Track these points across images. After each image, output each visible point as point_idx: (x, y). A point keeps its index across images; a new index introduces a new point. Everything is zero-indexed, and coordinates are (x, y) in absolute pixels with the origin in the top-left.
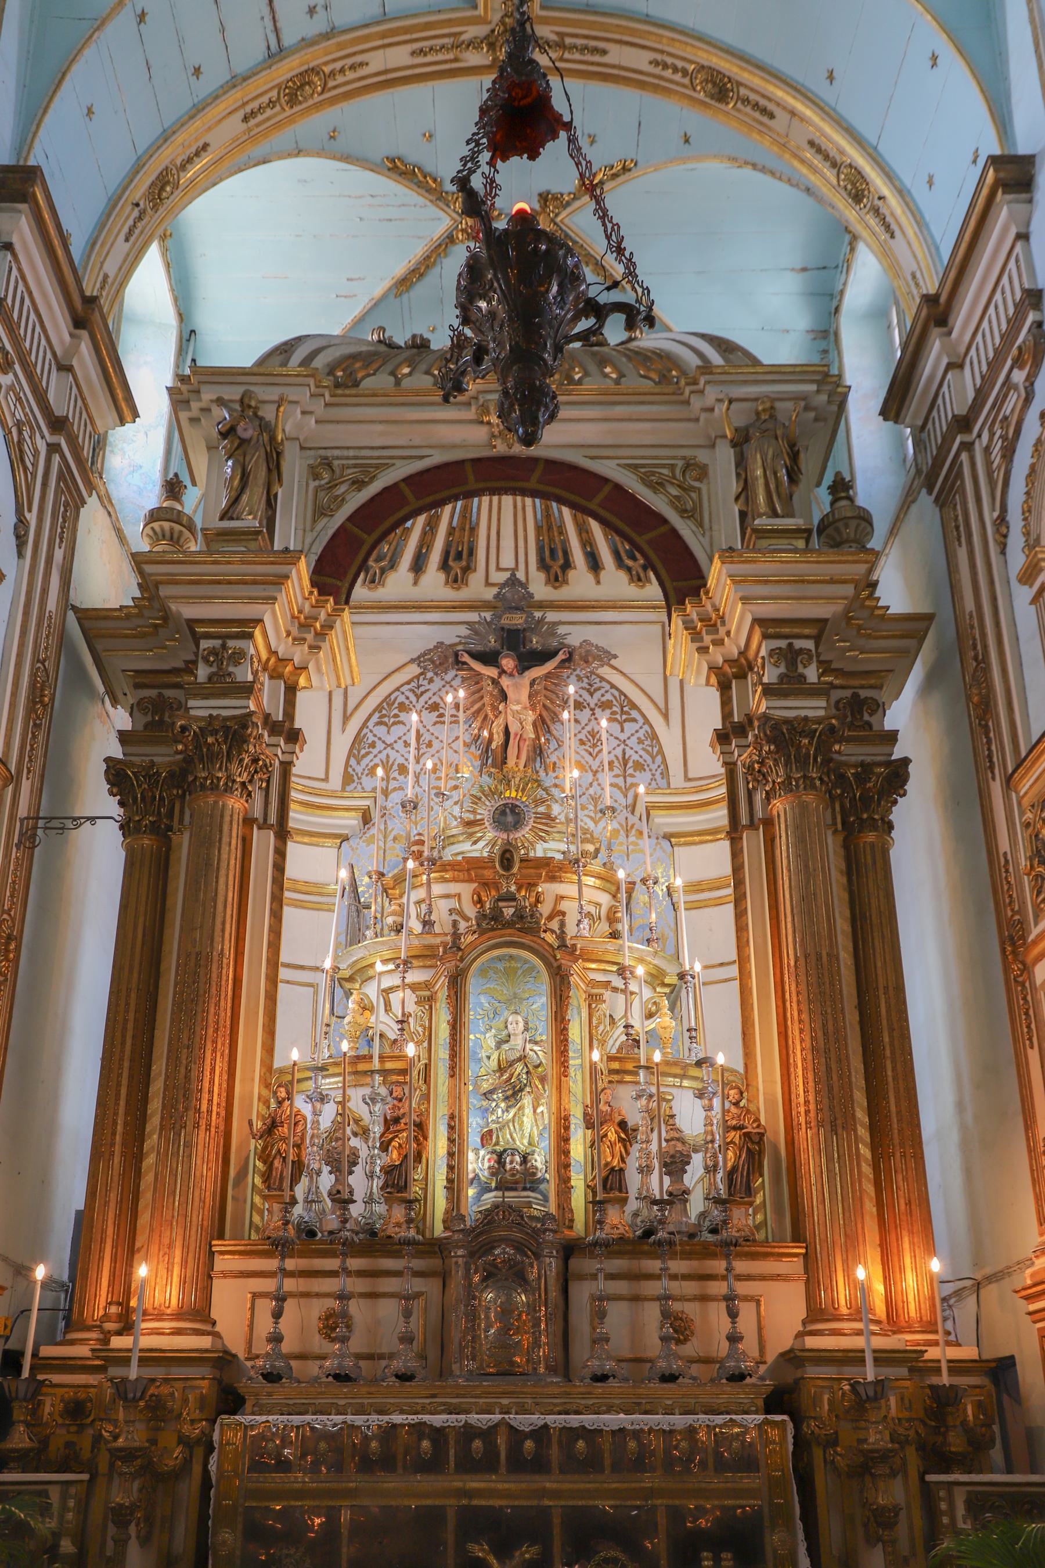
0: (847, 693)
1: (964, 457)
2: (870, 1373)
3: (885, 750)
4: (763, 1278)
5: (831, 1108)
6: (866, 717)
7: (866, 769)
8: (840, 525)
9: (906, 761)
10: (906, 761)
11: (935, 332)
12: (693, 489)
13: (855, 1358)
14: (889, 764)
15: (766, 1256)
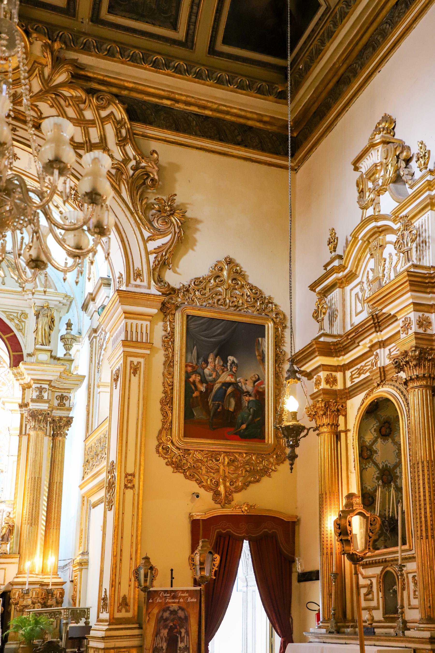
0: (60, 394)
1: (94, 340)
2: (27, 587)
3: (68, 412)
4: (7, 563)
5: (32, 520)
6: (64, 401)
7: (61, 418)
8: (66, 340)
9: (72, 418)
10: (72, 418)
11: (91, 303)
12: (24, 322)
13: (24, 584)
14: (67, 417)
15: (9, 558)
